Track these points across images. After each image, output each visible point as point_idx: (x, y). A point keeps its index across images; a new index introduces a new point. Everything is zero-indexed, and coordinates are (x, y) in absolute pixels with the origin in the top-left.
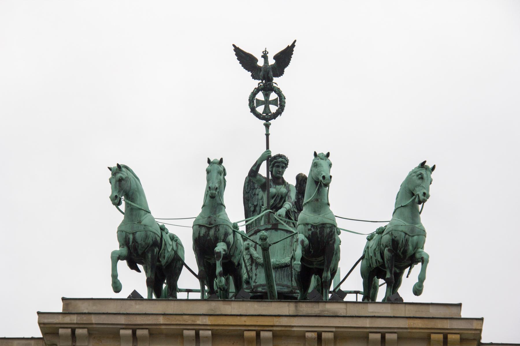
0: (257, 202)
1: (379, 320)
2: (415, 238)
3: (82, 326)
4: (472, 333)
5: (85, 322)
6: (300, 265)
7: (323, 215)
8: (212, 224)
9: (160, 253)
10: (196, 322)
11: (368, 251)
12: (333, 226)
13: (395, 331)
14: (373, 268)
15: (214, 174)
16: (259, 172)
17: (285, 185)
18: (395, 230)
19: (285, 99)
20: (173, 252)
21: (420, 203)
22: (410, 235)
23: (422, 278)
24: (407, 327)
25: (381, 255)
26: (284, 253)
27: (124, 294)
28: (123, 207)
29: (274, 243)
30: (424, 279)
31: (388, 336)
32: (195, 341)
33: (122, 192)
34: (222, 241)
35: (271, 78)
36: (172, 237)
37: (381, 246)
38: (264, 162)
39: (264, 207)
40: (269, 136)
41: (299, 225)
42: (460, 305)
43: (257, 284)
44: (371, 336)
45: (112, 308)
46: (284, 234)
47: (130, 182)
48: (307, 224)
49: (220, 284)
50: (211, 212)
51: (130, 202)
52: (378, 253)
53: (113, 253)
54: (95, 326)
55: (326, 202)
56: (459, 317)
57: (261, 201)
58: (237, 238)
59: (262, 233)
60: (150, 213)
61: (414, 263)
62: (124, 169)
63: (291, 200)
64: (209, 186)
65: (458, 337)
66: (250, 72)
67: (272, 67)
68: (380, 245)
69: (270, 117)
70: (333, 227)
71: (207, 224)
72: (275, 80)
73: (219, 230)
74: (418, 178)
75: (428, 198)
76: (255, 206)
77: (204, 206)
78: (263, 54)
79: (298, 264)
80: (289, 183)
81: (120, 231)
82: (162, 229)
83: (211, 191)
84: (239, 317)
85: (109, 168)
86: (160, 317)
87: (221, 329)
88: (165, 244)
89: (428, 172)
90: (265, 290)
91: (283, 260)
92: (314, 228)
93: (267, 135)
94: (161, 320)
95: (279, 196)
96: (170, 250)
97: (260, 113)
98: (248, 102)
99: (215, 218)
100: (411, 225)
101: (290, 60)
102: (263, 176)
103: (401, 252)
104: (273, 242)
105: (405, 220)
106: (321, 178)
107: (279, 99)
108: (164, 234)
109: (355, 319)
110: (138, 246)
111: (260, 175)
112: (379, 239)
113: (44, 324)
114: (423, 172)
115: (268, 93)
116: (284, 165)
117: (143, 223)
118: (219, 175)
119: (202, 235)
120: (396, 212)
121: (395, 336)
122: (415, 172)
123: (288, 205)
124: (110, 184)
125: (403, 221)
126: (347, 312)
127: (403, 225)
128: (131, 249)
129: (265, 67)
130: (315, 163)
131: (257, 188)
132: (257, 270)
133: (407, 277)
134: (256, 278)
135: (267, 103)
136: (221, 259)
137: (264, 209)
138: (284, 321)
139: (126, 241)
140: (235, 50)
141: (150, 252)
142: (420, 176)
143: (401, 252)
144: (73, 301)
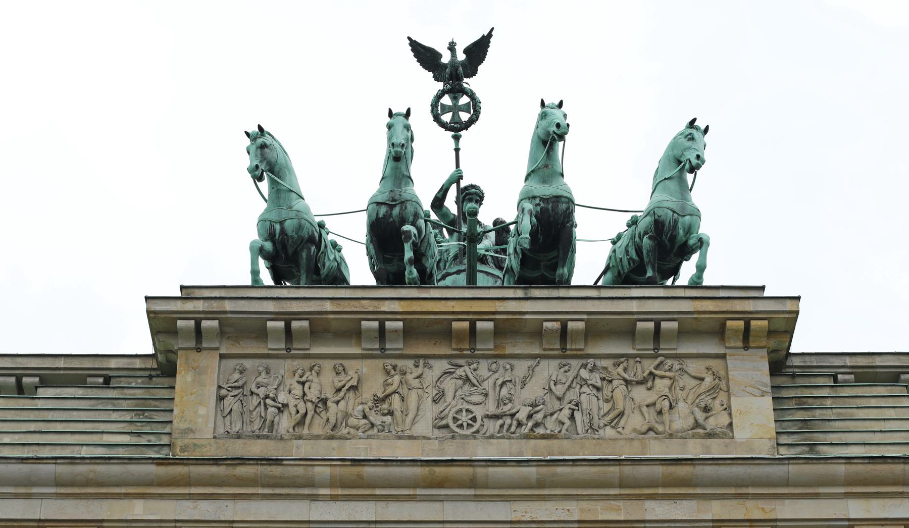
1: (650, 301)
2: (687, 218)
3: (210, 315)
4: (785, 318)
7: (556, 185)
8: (396, 201)
9: (318, 256)
12: (570, 201)
13: (675, 316)
14: (624, 275)
16: (446, 204)
19: (480, 103)
28: (264, 185)
30: (705, 267)
31: (664, 325)
32: (378, 339)
35: (460, 76)
36: (333, 245)
37: (637, 239)
40: (460, 152)
44: (640, 325)
48: (534, 198)
49: (411, 277)
50: (394, 185)
51: (276, 178)
52: (632, 249)
54: (229, 316)
57: (445, 254)
61: (685, 258)
70: (571, 204)
71: (388, 200)
72: (465, 80)
73: (406, 208)
74: (687, 139)
75: (703, 164)
77: (383, 178)
79: (527, 238)
81: (262, 220)
82: (321, 226)
83: (396, 149)
84: (443, 302)
88: (326, 247)
92: (543, 202)
93: (457, 150)
94: (328, 306)
96: (332, 258)
97: (447, 122)
98: (430, 109)
101: (486, 54)
103: (668, 237)
105: (671, 196)
106: (555, 129)
107: (471, 105)
109: (616, 302)
110: (288, 241)
112: (633, 231)
113: (155, 312)
114: (694, 131)
116: (478, 198)
117: (294, 208)
118: (406, 131)
119: (381, 216)
121: (675, 325)
122: (681, 134)
127: (669, 200)
128: (277, 245)
130: (543, 113)
135: (455, 109)
136: (411, 241)
140: (411, 44)
141: (305, 250)
143: (668, 237)
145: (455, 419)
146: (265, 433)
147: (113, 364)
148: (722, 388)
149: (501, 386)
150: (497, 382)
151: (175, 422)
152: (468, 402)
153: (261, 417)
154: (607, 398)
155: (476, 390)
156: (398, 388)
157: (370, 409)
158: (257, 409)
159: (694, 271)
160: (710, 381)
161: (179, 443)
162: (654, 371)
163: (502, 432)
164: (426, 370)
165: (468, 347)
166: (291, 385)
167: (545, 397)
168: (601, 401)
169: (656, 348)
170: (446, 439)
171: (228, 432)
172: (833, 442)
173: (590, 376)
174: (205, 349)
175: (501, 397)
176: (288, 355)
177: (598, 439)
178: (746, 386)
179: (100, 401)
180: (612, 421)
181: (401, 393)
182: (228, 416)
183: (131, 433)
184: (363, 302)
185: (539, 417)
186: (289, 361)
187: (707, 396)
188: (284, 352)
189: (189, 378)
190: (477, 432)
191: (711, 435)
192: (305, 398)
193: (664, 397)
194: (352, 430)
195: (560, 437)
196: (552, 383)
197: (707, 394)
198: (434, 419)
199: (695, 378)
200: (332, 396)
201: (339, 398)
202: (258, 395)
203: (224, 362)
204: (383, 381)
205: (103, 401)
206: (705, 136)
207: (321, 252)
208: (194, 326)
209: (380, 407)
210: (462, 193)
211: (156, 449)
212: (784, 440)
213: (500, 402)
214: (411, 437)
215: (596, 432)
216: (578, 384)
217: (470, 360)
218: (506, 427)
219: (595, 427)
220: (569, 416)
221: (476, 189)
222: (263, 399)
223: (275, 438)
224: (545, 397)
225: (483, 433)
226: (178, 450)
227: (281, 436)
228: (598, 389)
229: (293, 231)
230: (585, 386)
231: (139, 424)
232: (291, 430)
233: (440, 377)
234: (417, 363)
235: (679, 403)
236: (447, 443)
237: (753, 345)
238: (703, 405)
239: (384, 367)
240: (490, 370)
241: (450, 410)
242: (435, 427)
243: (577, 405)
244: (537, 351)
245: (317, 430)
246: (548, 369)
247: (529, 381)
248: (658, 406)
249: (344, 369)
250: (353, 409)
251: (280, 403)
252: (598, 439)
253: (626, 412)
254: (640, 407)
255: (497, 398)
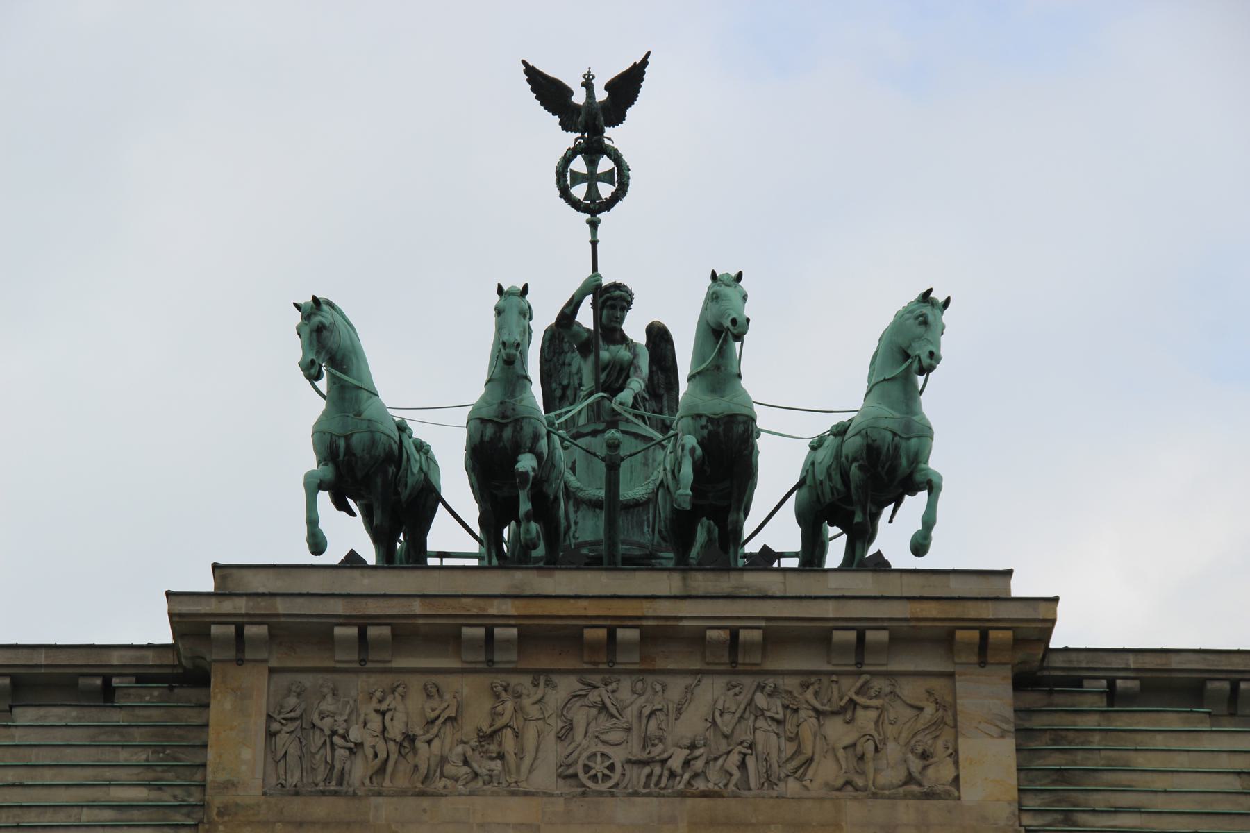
0: (569, 378)
1: (852, 602)
2: (914, 441)
3: (256, 619)
5: (263, 612)
6: (689, 497)
9: (398, 477)
10: (487, 609)
11: (814, 471)
12: (751, 419)
13: (885, 624)
15: (513, 316)
17: (627, 344)
18: (874, 427)
19: (629, 170)
20: (423, 475)
21: (921, 372)
22: (903, 435)
23: (929, 522)
24: (909, 616)
25: (842, 478)
26: (631, 479)
27: (333, 556)
28: (323, 384)
29: (631, 455)
30: (934, 523)
31: (870, 635)
33: (323, 353)
34: (527, 450)
35: (600, 128)
36: (418, 446)
37: (843, 459)
38: (588, 297)
39: (587, 390)
40: (598, 246)
41: (682, 417)
42: (1009, 573)
43: (580, 540)
44: (838, 636)
45: (315, 584)
46: (631, 443)
47: (338, 334)
48: (700, 416)
49: (528, 537)
51: (339, 374)
53: (309, 477)
54: (283, 619)
55: (737, 371)
56: (1008, 596)
57: (576, 378)
58: (554, 446)
59: (609, 435)
60: (378, 396)
62: (325, 307)
63: (642, 373)
64: (504, 339)
65: (1008, 635)
66: (557, 116)
67: (602, 106)
68: (841, 457)
69: (600, 207)
71: (497, 417)
72: (609, 131)
73: (521, 429)
74: (917, 322)
76: (565, 388)
77: (490, 381)
78: (584, 80)
79: (687, 495)
80: (634, 341)
82: (402, 428)
83: (508, 350)
84: (572, 601)
85: (295, 304)
86: (415, 601)
87: (538, 625)
88: (408, 459)
89: (937, 312)
90: (595, 553)
91: (630, 492)
92: (712, 423)
93: (594, 244)
94: (417, 607)
95: (616, 367)
96: (416, 470)
97: (579, 199)
98: (555, 178)
99: (514, 404)
100: (902, 416)
101: (639, 92)
102: (584, 326)
103: (885, 469)
104: (628, 454)
105: (892, 408)
107: (616, 172)
108: (405, 437)
109: (805, 603)
111: (579, 325)
112: (838, 446)
113: (180, 615)
114: (927, 310)
115: (594, 157)
116: (625, 304)
117: (366, 415)
118: (522, 319)
119: (487, 438)
120: (872, 392)
121: (883, 636)
122: (911, 312)
123: (636, 384)
124: (298, 336)
125: (890, 410)
126: (785, 590)
127: (889, 416)
129: (588, 107)
130: (714, 293)
131: (569, 351)
132: (579, 513)
133: (891, 521)
134: (576, 529)
135: (592, 178)
136: (529, 487)
137: (585, 393)
138: (665, 608)
139: (331, 453)
140: (526, 72)
142: (921, 319)
144: (235, 571)
145: (587, 768)
146: (332, 788)
147: (116, 658)
148: (948, 722)
149: (649, 717)
150: (644, 710)
151: (209, 769)
152: (604, 742)
153: (326, 762)
154: (790, 735)
155: (615, 724)
156: (511, 720)
157: (473, 750)
158: (322, 751)
159: (919, 526)
160: (930, 713)
161: (217, 801)
162: (855, 697)
163: (649, 787)
164: (549, 691)
165: (605, 660)
166: (366, 715)
167: (707, 734)
168: (783, 740)
169: (860, 663)
170: (574, 796)
171: (283, 786)
172: (1097, 809)
173: (768, 704)
174: (249, 661)
175: (648, 733)
176: (362, 667)
177: (777, 797)
178: (980, 722)
179: (103, 730)
180: (797, 769)
181: (515, 727)
182: (282, 761)
183: (150, 785)
184: (464, 600)
185: (698, 765)
186: (363, 677)
187: (926, 735)
188: (356, 665)
189: (228, 706)
190: (617, 785)
191: (929, 795)
192: (386, 735)
193: (868, 737)
194: (449, 783)
195: (726, 795)
196: (717, 714)
197: (927, 732)
198: (559, 764)
199: (912, 706)
200: (421, 732)
201: (432, 736)
202: (322, 730)
203: (276, 677)
204: (490, 706)
205: (107, 729)
206: (945, 312)
207: (401, 471)
208: (234, 634)
209: (487, 746)
210: (601, 296)
211: (185, 810)
212: (1032, 802)
213: (646, 742)
214: (527, 794)
215: (775, 787)
216: (752, 715)
217: (607, 676)
218: (654, 779)
219: (774, 779)
220: (738, 763)
221: (622, 291)
222: (329, 736)
223: (346, 794)
224: (707, 734)
225: (625, 785)
226: (215, 811)
227: (354, 791)
228: (778, 722)
229: (363, 450)
230: (761, 718)
231: (159, 769)
232: (367, 782)
233: (567, 703)
234: (536, 680)
235: (888, 744)
236: (576, 802)
237: (992, 661)
238: (920, 750)
239: (492, 688)
240: (634, 692)
241: (580, 754)
242: (559, 776)
243: (750, 747)
244: (697, 667)
245: (402, 782)
246: (712, 691)
247: (687, 708)
248: (859, 749)
249: (438, 691)
250: (451, 750)
251: (351, 742)
252: (777, 797)
253: (816, 757)
254: (834, 749)
255: (643, 735)
